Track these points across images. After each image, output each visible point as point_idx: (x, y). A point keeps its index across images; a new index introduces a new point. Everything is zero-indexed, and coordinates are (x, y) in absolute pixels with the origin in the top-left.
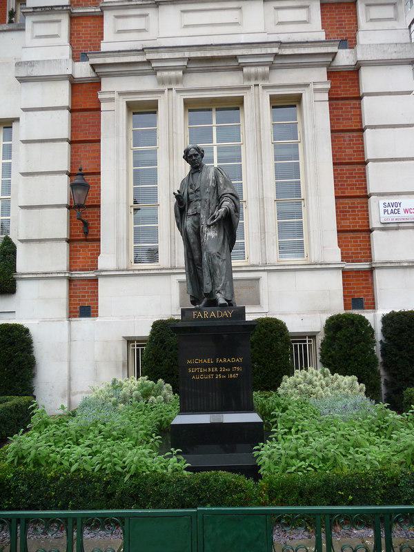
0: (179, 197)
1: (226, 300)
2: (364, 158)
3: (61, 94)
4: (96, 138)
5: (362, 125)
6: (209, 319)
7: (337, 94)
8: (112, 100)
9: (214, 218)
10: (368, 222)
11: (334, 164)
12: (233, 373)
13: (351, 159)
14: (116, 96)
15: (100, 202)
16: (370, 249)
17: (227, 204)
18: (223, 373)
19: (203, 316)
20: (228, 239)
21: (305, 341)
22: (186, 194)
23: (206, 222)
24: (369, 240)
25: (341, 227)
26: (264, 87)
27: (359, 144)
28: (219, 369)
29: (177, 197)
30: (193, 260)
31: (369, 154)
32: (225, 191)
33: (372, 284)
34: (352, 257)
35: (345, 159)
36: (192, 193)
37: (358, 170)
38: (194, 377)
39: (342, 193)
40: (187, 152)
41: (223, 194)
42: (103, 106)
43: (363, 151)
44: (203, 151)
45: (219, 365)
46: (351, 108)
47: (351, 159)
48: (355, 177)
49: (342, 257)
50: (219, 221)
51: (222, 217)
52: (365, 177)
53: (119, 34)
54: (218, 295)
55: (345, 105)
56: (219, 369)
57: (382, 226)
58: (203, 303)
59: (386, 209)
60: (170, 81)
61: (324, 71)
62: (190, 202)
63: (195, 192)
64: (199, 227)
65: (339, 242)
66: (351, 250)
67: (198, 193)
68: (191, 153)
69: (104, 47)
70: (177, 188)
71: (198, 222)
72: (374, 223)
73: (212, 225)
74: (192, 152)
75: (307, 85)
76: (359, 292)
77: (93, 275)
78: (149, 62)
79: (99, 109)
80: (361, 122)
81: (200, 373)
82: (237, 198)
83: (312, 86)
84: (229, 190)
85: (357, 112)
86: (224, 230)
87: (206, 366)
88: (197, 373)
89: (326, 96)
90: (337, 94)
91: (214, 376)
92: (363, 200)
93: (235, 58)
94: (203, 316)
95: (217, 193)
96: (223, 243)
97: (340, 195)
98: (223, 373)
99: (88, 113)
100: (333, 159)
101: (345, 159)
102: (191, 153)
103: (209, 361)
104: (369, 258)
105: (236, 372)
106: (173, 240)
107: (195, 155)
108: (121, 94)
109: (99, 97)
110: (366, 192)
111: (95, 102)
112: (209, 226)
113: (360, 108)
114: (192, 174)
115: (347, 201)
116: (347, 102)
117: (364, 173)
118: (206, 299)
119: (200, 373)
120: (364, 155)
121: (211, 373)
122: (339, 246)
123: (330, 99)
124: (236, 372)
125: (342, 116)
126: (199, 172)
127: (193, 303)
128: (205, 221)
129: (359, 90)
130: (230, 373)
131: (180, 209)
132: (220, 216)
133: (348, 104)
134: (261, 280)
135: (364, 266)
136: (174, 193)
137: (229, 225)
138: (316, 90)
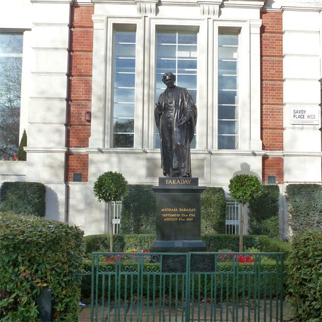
2: (282, 77)
45: (180, 213)
55: (272, 37)
98: (183, 218)
101: (269, 77)
105: (191, 217)
114: (166, 92)
121: (176, 217)
125: (268, 45)
130: (187, 217)
133: (275, 37)
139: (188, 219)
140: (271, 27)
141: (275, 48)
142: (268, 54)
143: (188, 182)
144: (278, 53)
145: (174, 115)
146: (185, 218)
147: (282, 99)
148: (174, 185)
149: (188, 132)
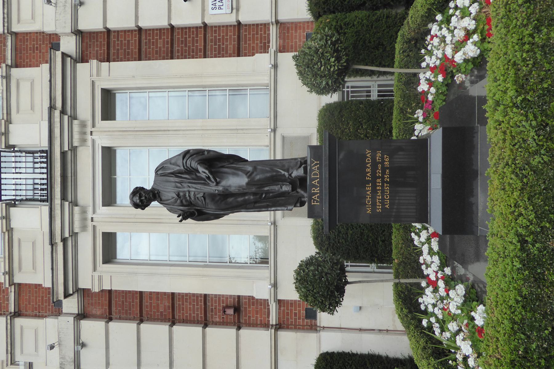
0: (185, 216)
1: (300, 167)
2: (168, 29)
3: (92, 328)
4: (138, 295)
5: (135, 31)
6: (320, 187)
7: (104, 53)
8: (100, 278)
9: (208, 178)
10: (231, 26)
11: (172, 58)
12: (383, 161)
13: (168, 42)
14: (96, 275)
15: (201, 295)
16: (257, 25)
17: (194, 164)
18: (384, 173)
19: (317, 193)
20: (232, 163)
21: (348, 92)
22: (181, 208)
24: (249, 26)
25: (234, 53)
26: (94, 126)
27: (153, 33)
28: (379, 177)
29: (185, 218)
31: (164, 23)
33: (292, 23)
34: (265, 43)
35: (167, 48)
36: (182, 202)
37: (178, 35)
38: (387, 206)
39: (200, 52)
40: (136, 206)
41: (184, 167)
42: (107, 287)
43: (160, 29)
45: (374, 177)
46: (118, 40)
47: (168, 42)
48: (186, 38)
49: (265, 52)
50: (211, 172)
51: (206, 169)
52: (186, 28)
53: (37, 270)
54: (293, 175)
56: (379, 177)
57: (234, 11)
58: (302, 192)
59: (217, 7)
60: (84, 219)
61: (79, 66)
62: (190, 204)
63: (180, 198)
64: (219, 195)
65: (249, 56)
66: (257, 44)
67: (181, 194)
69: (48, 284)
70: (174, 217)
71: (212, 196)
72: (231, 19)
73: (216, 180)
74: (137, 199)
75: (93, 83)
76: (300, 37)
77: (274, 305)
78: (64, 240)
79: (110, 291)
80: (131, 31)
81: (383, 199)
83: (94, 78)
84: (180, 162)
85: (121, 35)
86: (223, 167)
87: (374, 191)
88: (383, 204)
89: (105, 65)
90: (104, 53)
91: (387, 182)
92: (209, 31)
93: (63, 154)
97: (202, 53)
98: (384, 173)
99: (113, 302)
100: (167, 59)
103: (369, 188)
104: (265, 26)
105: (382, 158)
106: (241, 222)
107: (140, 197)
108: (95, 269)
109: (96, 290)
110: (200, 27)
111: (102, 295)
112: (218, 184)
113: (118, 31)
114: (161, 201)
115: (209, 47)
116: (112, 45)
117: (182, 28)
118: (299, 190)
119: (383, 199)
120: (164, 29)
121: (383, 186)
122: (253, 55)
123: (108, 60)
124: (382, 158)
125: (125, 50)
126: (159, 193)
127: (302, 204)
128: (212, 188)
129: (101, 32)
130: (383, 165)
131: (199, 215)
132: (207, 172)
133: (114, 41)
134: (285, 135)
135: (273, 31)
136: (181, 221)
138: (98, 74)
139: (387, 164)
140: (101, 48)
141: (128, 41)
142: (137, 50)
143: (316, 164)
144: (135, 37)
145: (195, 191)
146: (384, 169)
147: (197, 28)
148: (321, 190)
149: (225, 164)
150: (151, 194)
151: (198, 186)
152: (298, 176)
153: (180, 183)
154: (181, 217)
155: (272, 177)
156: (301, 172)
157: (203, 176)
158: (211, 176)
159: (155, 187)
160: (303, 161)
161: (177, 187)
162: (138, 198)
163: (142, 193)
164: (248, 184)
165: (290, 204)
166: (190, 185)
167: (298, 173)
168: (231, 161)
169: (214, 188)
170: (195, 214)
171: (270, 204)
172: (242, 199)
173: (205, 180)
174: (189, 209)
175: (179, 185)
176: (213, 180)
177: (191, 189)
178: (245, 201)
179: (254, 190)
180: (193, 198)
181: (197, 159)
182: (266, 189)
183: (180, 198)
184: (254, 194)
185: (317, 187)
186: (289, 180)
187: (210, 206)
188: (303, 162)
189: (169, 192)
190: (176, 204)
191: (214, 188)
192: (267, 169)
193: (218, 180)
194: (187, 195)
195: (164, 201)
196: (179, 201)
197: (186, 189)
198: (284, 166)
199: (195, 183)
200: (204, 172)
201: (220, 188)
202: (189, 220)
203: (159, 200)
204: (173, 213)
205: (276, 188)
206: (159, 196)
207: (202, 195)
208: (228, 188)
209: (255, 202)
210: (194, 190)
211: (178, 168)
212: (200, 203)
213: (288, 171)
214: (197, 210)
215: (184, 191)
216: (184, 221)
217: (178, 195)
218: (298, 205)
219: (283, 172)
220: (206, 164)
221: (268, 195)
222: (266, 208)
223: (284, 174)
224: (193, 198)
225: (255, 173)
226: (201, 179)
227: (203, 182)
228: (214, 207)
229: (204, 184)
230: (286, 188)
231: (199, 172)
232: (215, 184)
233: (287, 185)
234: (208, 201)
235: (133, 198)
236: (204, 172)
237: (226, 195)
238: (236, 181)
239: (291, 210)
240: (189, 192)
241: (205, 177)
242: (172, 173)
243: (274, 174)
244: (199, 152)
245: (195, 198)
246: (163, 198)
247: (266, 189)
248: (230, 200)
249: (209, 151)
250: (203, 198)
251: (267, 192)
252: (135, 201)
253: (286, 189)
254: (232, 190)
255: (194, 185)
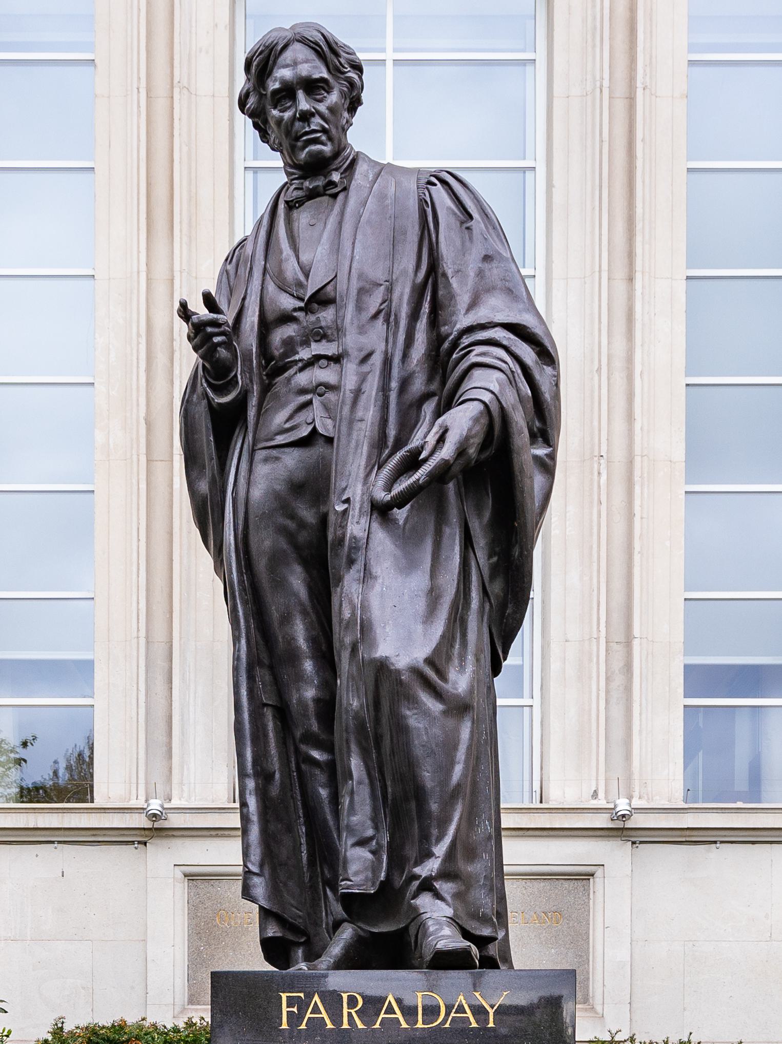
9: (413, 462)
22: (252, 319)
23: (367, 490)
29: (201, 335)
30: (283, 713)
32: (482, 314)
36: (286, 318)
40: (261, 64)
41: (470, 330)
44: (358, 68)
50: (441, 475)
51: (461, 452)
54: (425, 902)
58: (336, 949)
62: (274, 366)
63: (307, 309)
67: (326, 316)
68: (283, 73)
71: (314, 486)
82: (547, 356)
84: (495, 309)
86: (468, 542)
94: (336, 1017)
95: (434, 322)
96: (457, 619)
102: (283, 73)
107: (313, 86)
112: (381, 511)
114: (284, 206)
118: (347, 933)
126: (331, 192)
127: (273, 950)
128: (358, 483)
131: (215, 412)
132: (447, 452)
136: (185, 312)
137: (490, 500)
145: (346, 389)
149: (481, 555)
150: (327, 149)
151: (369, 413)
152: (422, 926)
153: (386, 314)
154: (200, 310)
155: (419, 794)
156: (444, 936)
157: (423, 436)
158: (420, 474)
159: (361, 168)
160: (493, 950)
161: (362, 291)
162: (304, 70)
163: (334, 97)
164: (382, 668)
165: (275, 890)
166: (377, 360)
167: (439, 921)
168: (496, 588)
169: (356, 492)
170: (220, 390)
171: (275, 790)
172: (302, 642)
173: (399, 443)
174: (247, 358)
175: (374, 302)
176: (401, 486)
177: (351, 368)
178: (293, 657)
179: (352, 701)
180: (303, 379)
181: (510, 399)
182: (356, 764)
183: (307, 309)
184: (327, 706)
185: (369, 1022)
186: (399, 882)
187: (262, 470)
188: (482, 953)
189: (336, 248)
190: (271, 287)
191: (356, 492)
192: (458, 770)
193: (401, 514)
194: (318, 348)
195: (289, 221)
196: (287, 303)
197: (352, 340)
198: (471, 854)
199: (384, 389)
200: (441, 440)
201: (356, 527)
202: (187, 360)
203: (292, 194)
204: (224, 272)
205: (359, 811)
206: (313, 194)
207: (325, 426)
208: (359, 566)
209: (283, 713)
210: (350, 382)
211: (463, 299)
212: (279, 418)
213: (446, 874)
214: (241, 404)
215: (339, 330)
216: (182, 329)
217: (321, 299)
218: (273, 931)
219: (440, 850)
220: (484, 446)
221: (321, 777)
222: (256, 771)
223: (429, 855)
224: (303, 379)
225: (435, 706)
226: (407, 427)
227: (392, 432)
228: (257, 493)
229: (380, 442)
230: (359, 868)
231: (438, 414)
232: (382, 495)
233: (375, 869)
234: (291, 459)
235: (303, 41)
236: (441, 440)
237: (321, 557)
238: (396, 607)
239: (247, 893)
240: (336, 359)
241: (415, 442)
242: (434, 268)
243: (434, 807)
244: (544, 420)
245: (303, 391)
246: (303, 217)
247: (356, 764)
248: (297, 581)
249: (547, 467)
250: (305, 431)
251: (335, 774)
252: (288, 56)
253: (353, 868)
254: (350, 587)
255: (372, 386)
